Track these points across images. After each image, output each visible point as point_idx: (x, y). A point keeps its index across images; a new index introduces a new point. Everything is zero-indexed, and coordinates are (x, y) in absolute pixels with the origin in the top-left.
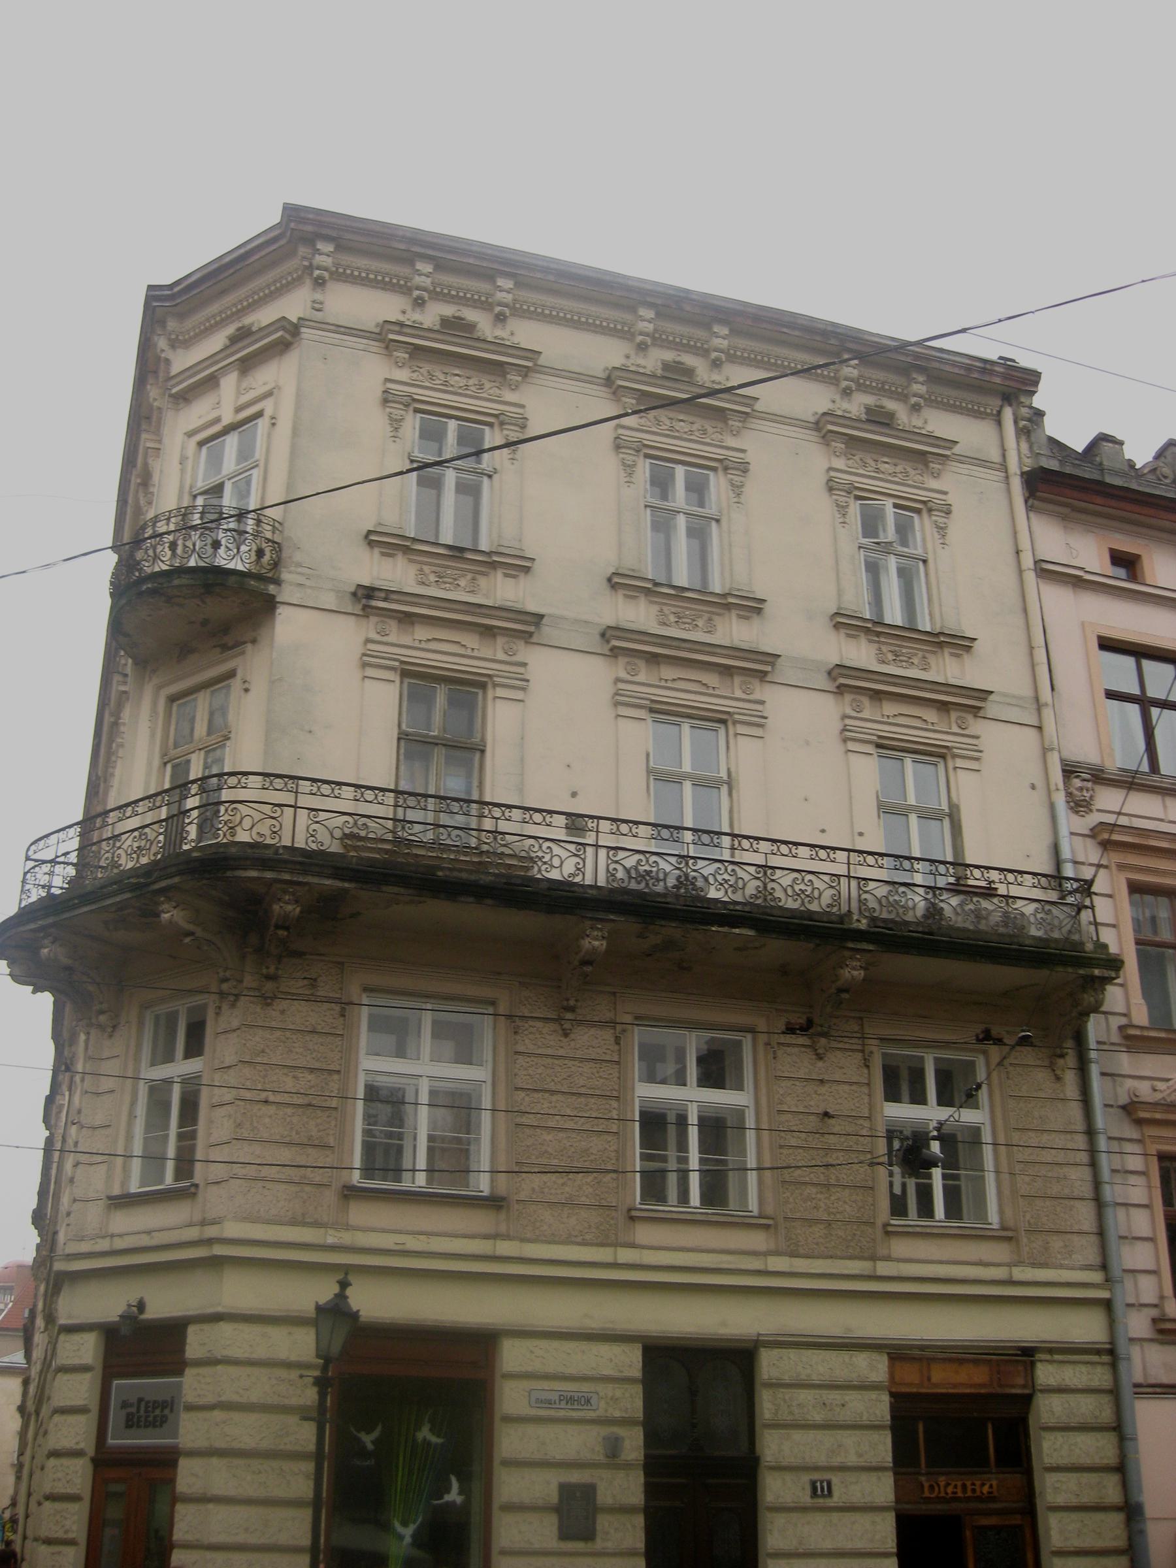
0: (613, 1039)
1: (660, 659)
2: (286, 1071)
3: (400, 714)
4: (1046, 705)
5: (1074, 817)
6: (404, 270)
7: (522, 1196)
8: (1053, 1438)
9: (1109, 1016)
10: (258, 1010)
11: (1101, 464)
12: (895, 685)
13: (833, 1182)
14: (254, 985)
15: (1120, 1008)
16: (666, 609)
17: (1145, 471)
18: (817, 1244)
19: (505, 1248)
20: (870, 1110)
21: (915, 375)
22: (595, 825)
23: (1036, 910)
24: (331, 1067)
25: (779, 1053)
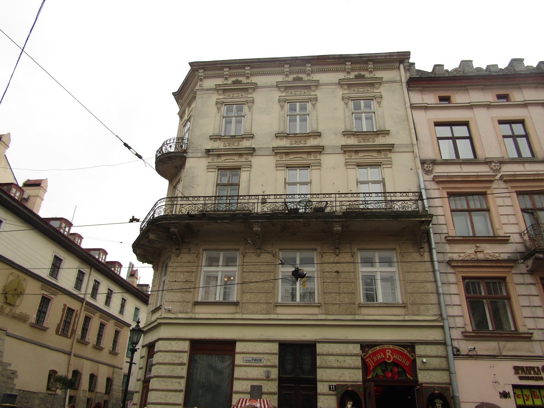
1: (289, 153)
2: (181, 273)
3: (217, 179)
4: (414, 145)
6: (221, 72)
7: (244, 301)
9: (441, 235)
10: (175, 258)
11: (435, 73)
12: (361, 147)
14: (175, 252)
15: (445, 232)
16: (292, 141)
18: (336, 311)
21: (369, 63)
25: (324, 255)
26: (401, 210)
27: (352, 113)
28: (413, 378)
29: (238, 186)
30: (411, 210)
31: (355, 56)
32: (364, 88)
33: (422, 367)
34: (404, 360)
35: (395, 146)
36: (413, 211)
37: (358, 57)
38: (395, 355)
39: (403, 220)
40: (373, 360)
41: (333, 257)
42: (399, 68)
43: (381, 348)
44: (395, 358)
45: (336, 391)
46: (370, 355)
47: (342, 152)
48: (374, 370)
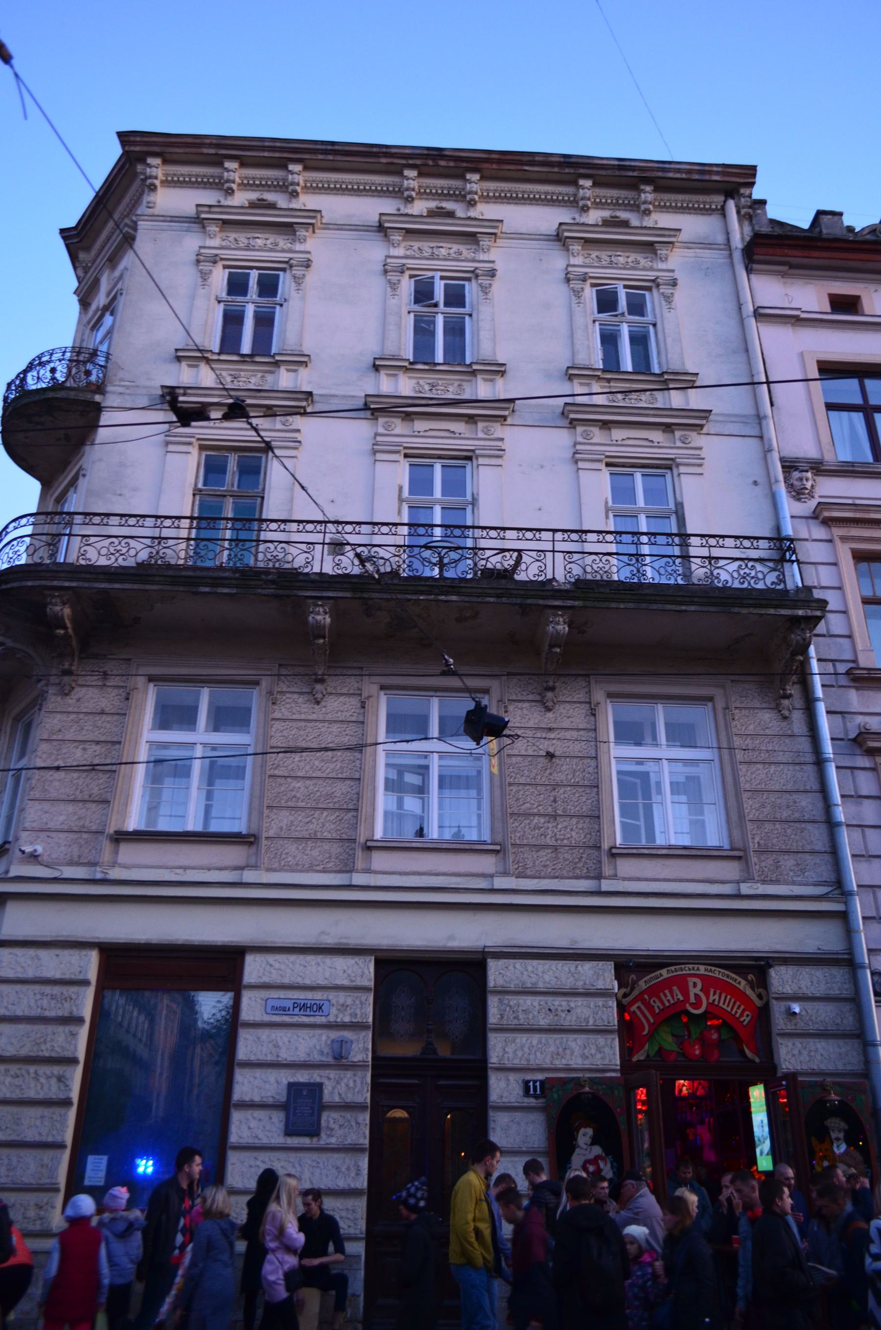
0: (359, 705)
2: (76, 744)
3: (197, 477)
5: (797, 505)
7: (271, 833)
8: (790, 1044)
13: (560, 812)
15: (848, 656)
16: (422, 382)
17: (865, 233)
19: (249, 876)
20: (596, 751)
21: (642, 187)
22: (323, 528)
23: (740, 567)
24: (115, 739)
26: (736, 585)
27: (594, 321)
28: (759, 1057)
29: (259, 499)
30: (764, 587)
31: (605, 162)
32: (627, 254)
33: (789, 1027)
34: (738, 1008)
35: (712, 417)
36: (768, 590)
37: (613, 165)
38: (714, 994)
39: (744, 611)
40: (651, 1009)
41: (535, 715)
42: (722, 212)
43: (675, 974)
44: (714, 1000)
45: (545, 1097)
46: (642, 993)
47: (566, 423)
48: (651, 1035)
